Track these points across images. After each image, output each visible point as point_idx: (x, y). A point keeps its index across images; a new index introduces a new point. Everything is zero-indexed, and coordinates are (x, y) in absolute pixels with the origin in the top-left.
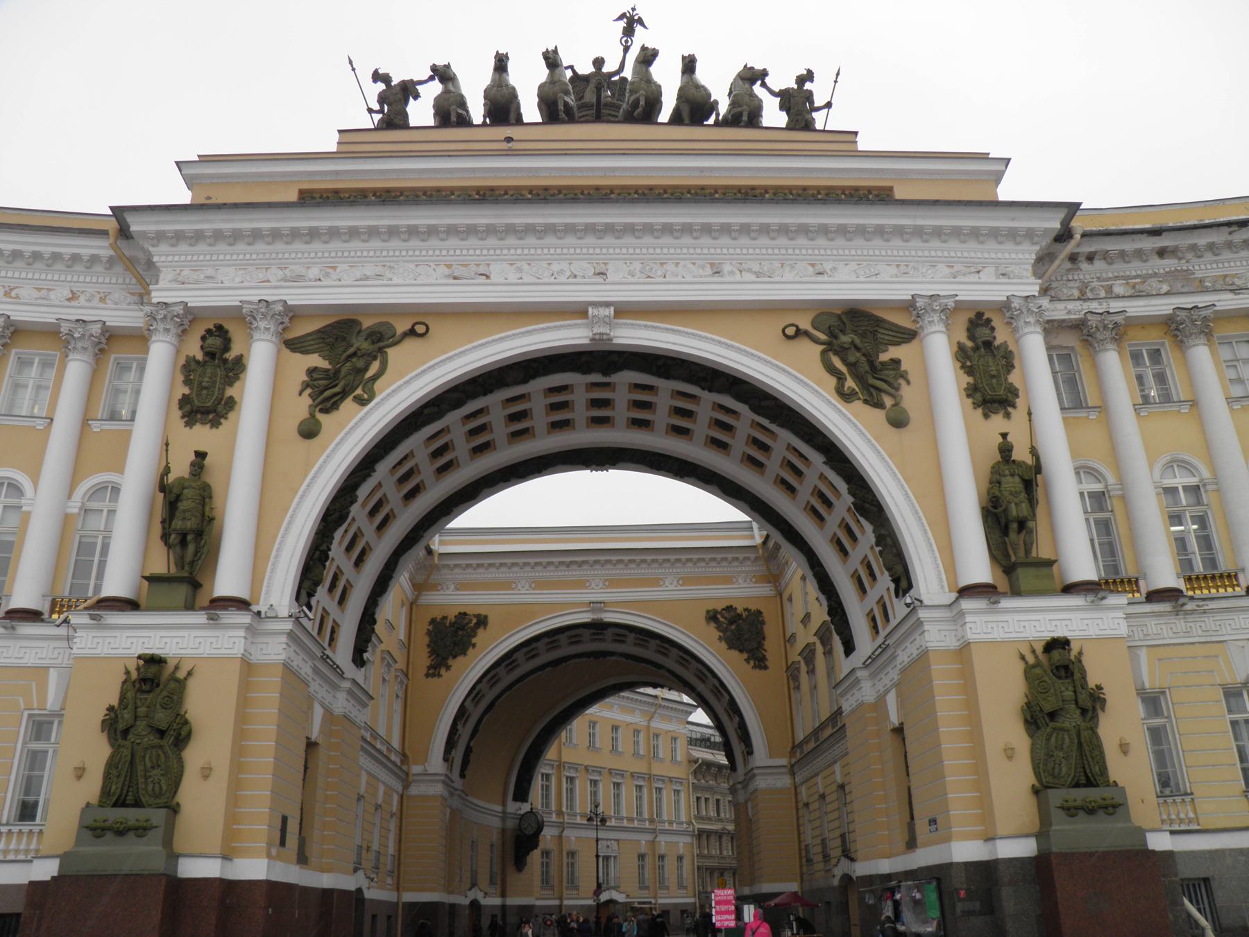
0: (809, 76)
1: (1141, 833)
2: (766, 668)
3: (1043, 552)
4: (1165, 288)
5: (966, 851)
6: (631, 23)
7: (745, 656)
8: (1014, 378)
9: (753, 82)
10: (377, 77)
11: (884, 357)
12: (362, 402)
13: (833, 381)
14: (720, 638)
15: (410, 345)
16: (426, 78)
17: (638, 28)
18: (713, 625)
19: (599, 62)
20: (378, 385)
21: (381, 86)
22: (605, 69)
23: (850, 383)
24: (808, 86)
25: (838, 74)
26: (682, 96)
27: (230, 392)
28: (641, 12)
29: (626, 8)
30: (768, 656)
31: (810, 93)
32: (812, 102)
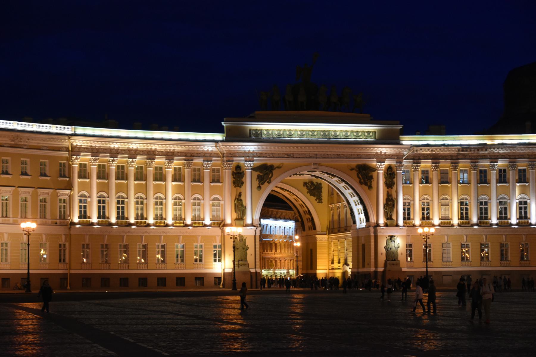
1: (401, 268)
2: (322, 202)
3: (394, 217)
4: (431, 158)
5: (373, 269)
7: (315, 198)
8: (395, 180)
11: (369, 175)
12: (269, 182)
13: (358, 180)
14: (308, 193)
15: (277, 169)
18: (305, 187)
20: (272, 179)
23: (362, 181)
27: (243, 179)
30: (323, 198)
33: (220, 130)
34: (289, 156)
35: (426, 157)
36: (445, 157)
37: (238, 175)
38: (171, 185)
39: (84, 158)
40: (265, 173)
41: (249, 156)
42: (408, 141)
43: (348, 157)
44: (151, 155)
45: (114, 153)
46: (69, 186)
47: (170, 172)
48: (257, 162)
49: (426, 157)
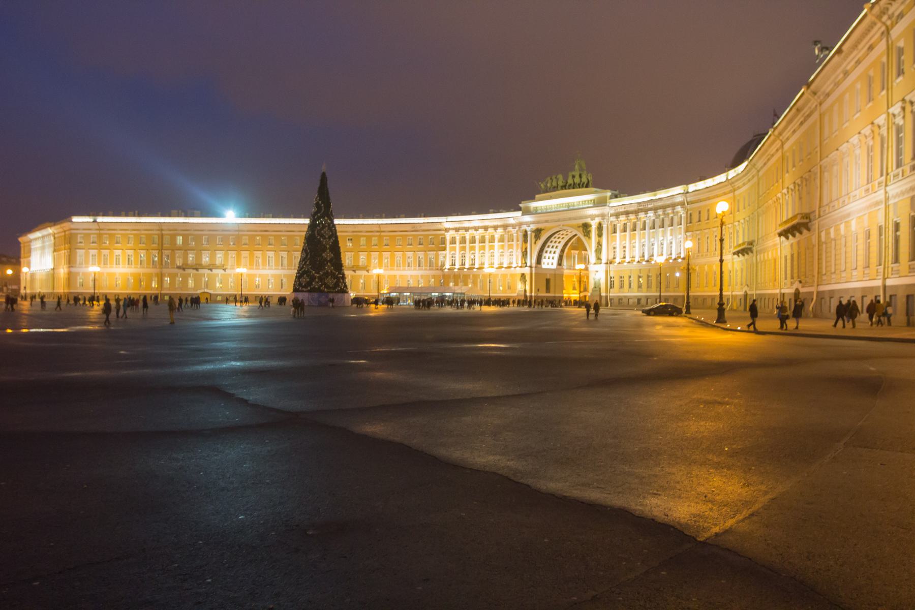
33: (519, 209)
34: (547, 221)
35: (622, 213)
36: (632, 212)
37: (525, 235)
38: (497, 244)
39: (452, 233)
40: (538, 232)
41: (528, 224)
42: (615, 203)
43: (575, 219)
44: (486, 228)
45: (467, 229)
46: (444, 249)
47: (497, 236)
48: (533, 227)
49: (622, 213)
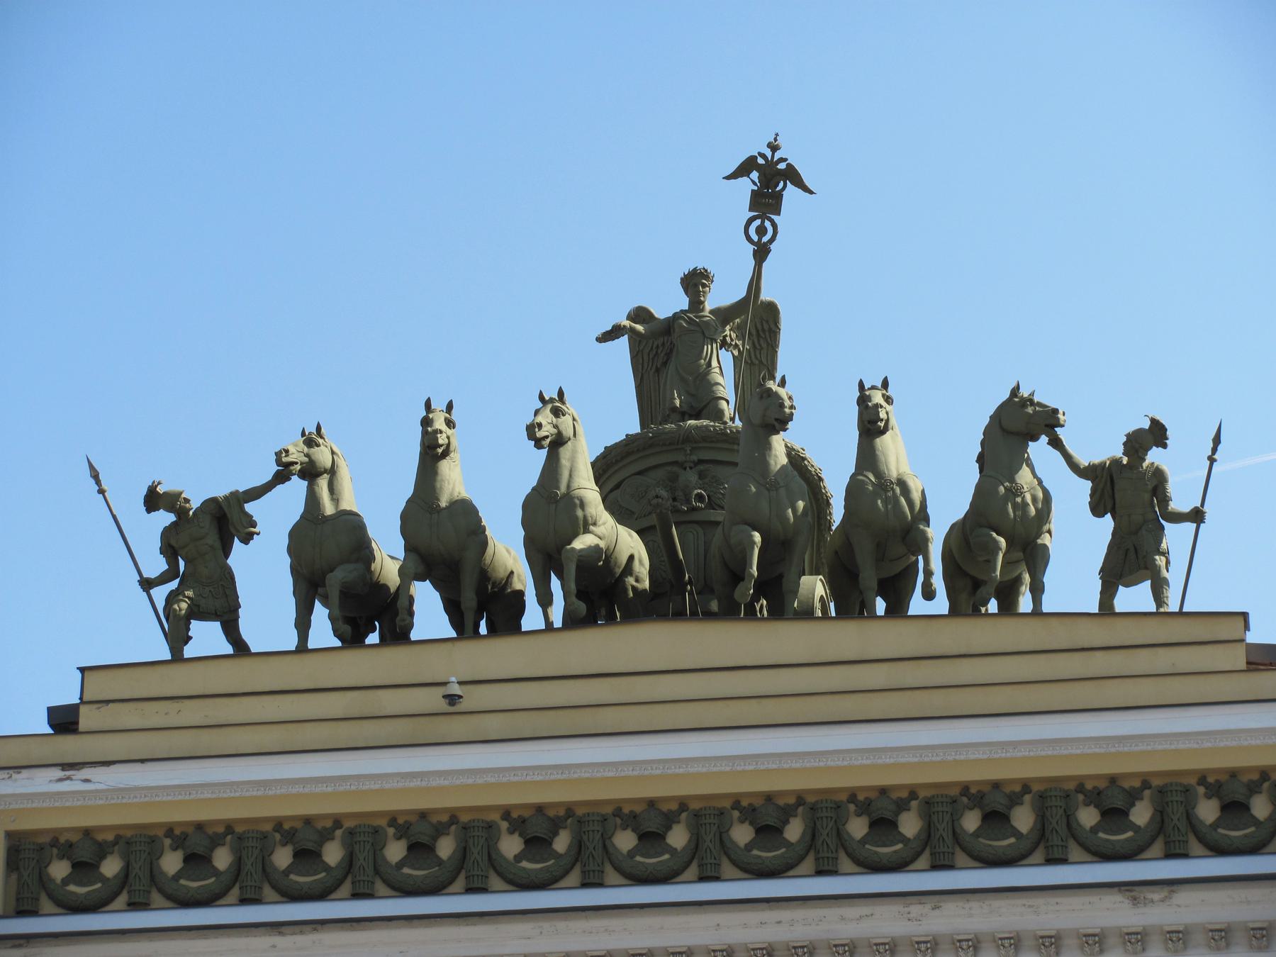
0: (1156, 434)
6: (770, 181)
9: (1035, 438)
10: (153, 500)
16: (268, 477)
17: (791, 193)
19: (695, 282)
21: (165, 518)
22: (719, 296)
24: (1155, 456)
25: (1217, 440)
26: (854, 490)
28: (791, 153)
29: (757, 147)
31: (1159, 477)
32: (1165, 500)
